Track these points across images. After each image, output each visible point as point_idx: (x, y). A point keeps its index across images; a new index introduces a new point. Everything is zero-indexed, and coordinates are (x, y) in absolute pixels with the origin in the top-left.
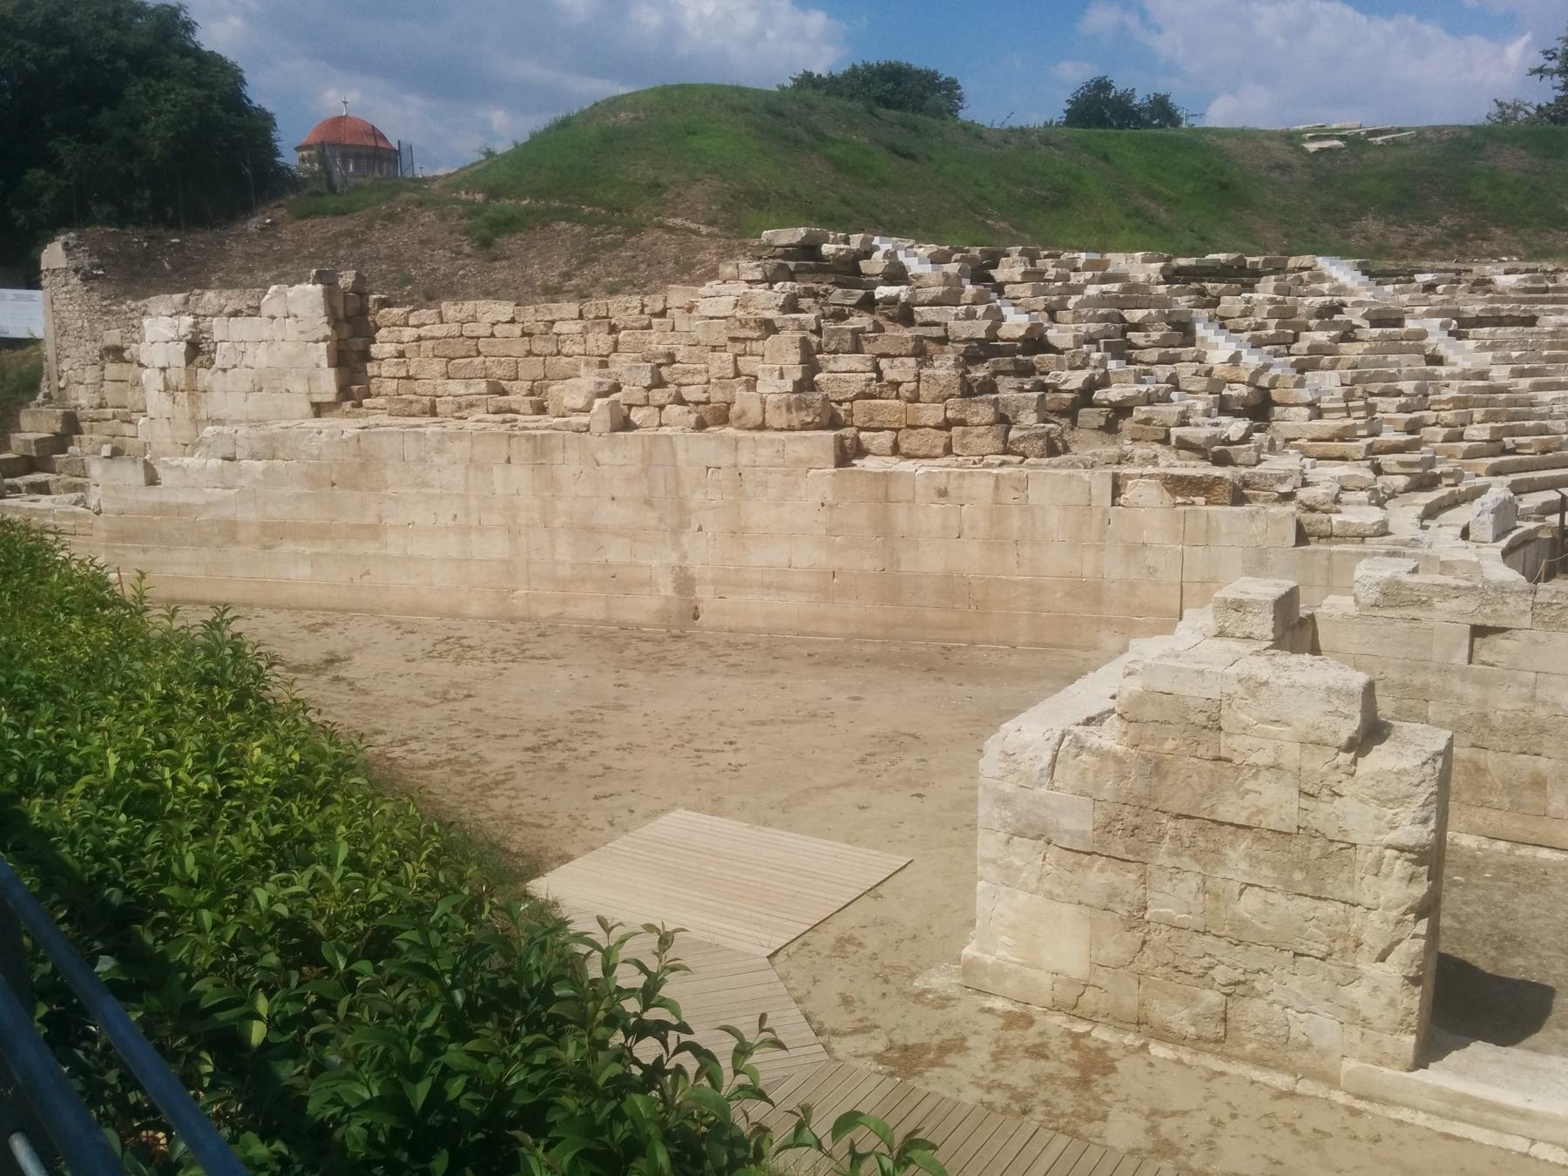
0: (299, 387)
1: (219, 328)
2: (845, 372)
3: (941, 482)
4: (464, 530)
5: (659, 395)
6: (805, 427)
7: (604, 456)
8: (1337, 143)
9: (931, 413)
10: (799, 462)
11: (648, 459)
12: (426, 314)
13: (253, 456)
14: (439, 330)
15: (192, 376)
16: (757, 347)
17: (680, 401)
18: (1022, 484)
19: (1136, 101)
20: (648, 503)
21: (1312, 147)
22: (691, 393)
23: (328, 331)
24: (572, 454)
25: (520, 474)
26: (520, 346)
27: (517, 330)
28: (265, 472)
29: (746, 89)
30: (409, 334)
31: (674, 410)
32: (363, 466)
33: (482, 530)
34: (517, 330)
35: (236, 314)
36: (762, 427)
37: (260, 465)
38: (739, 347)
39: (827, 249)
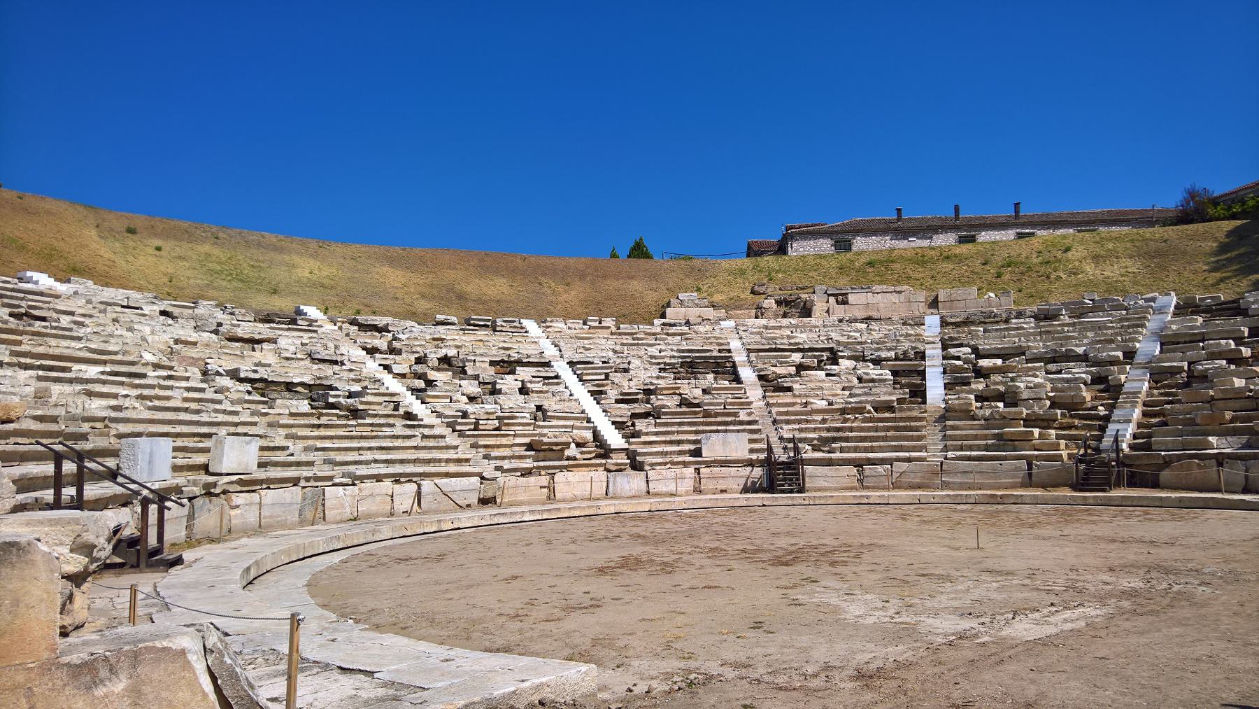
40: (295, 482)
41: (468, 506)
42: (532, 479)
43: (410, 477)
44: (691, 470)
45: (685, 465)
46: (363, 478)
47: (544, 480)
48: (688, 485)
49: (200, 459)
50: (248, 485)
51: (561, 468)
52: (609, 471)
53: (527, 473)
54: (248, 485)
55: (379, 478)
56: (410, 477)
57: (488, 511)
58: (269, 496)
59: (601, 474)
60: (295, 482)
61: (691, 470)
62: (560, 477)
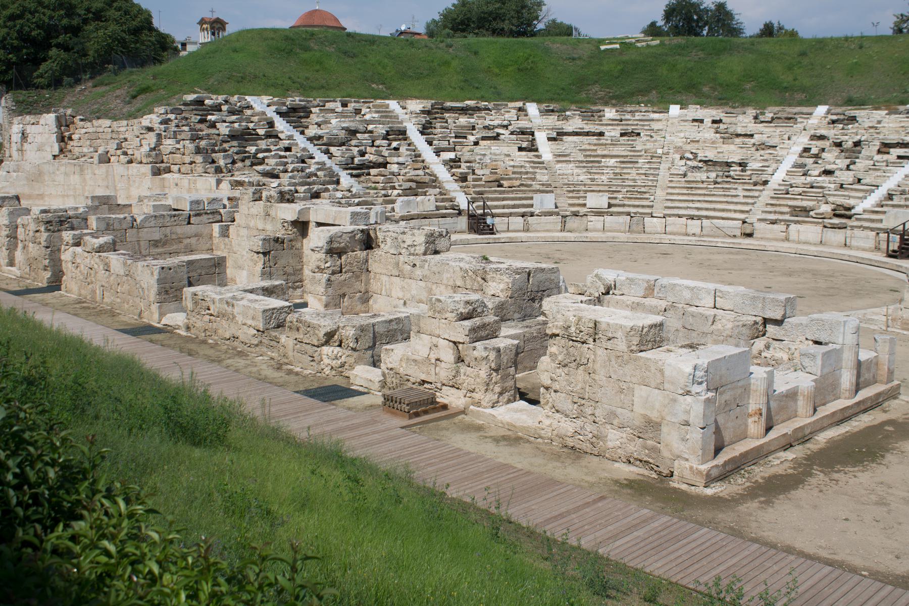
0: (49, 149)
1: (30, 129)
2: (168, 144)
3: (176, 181)
4: (63, 196)
5: (119, 152)
6: (151, 163)
7: (97, 172)
8: (618, 46)
9: (187, 159)
10: (143, 174)
11: (107, 171)
12: (88, 124)
13: (14, 171)
14: (91, 130)
15: (22, 145)
16: (146, 136)
17: (125, 154)
18: (195, 182)
19: (705, 5)
20: (107, 187)
21: (603, 48)
22: (130, 152)
23: (56, 130)
24: (89, 171)
25: (77, 177)
26: (109, 137)
27: (110, 130)
28: (17, 176)
29: (278, 30)
30: (84, 131)
31: (122, 157)
32: (40, 174)
33: (67, 196)
34: (110, 130)
35: (33, 124)
36: (141, 163)
37: (15, 174)
38: (141, 136)
39: (207, 102)
40: (628, 214)
41: (735, 236)
42: (775, 226)
43: (699, 218)
44: (874, 233)
45: (872, 229)
46: (670, 216)
47: (782, 227)
48: (871, 244)
49: (581, 201)
50: (599, 213)
51: (796, 222)
52: (825, 227)
53: (773, 222)
54: (599, 213)
55: (680, 216)
56: (699, 218)
57: (748, 241)
58: (608, 219)
59: (819, 228)
60: (628, 214)
61: (874, 233)
62: (793, 227)
